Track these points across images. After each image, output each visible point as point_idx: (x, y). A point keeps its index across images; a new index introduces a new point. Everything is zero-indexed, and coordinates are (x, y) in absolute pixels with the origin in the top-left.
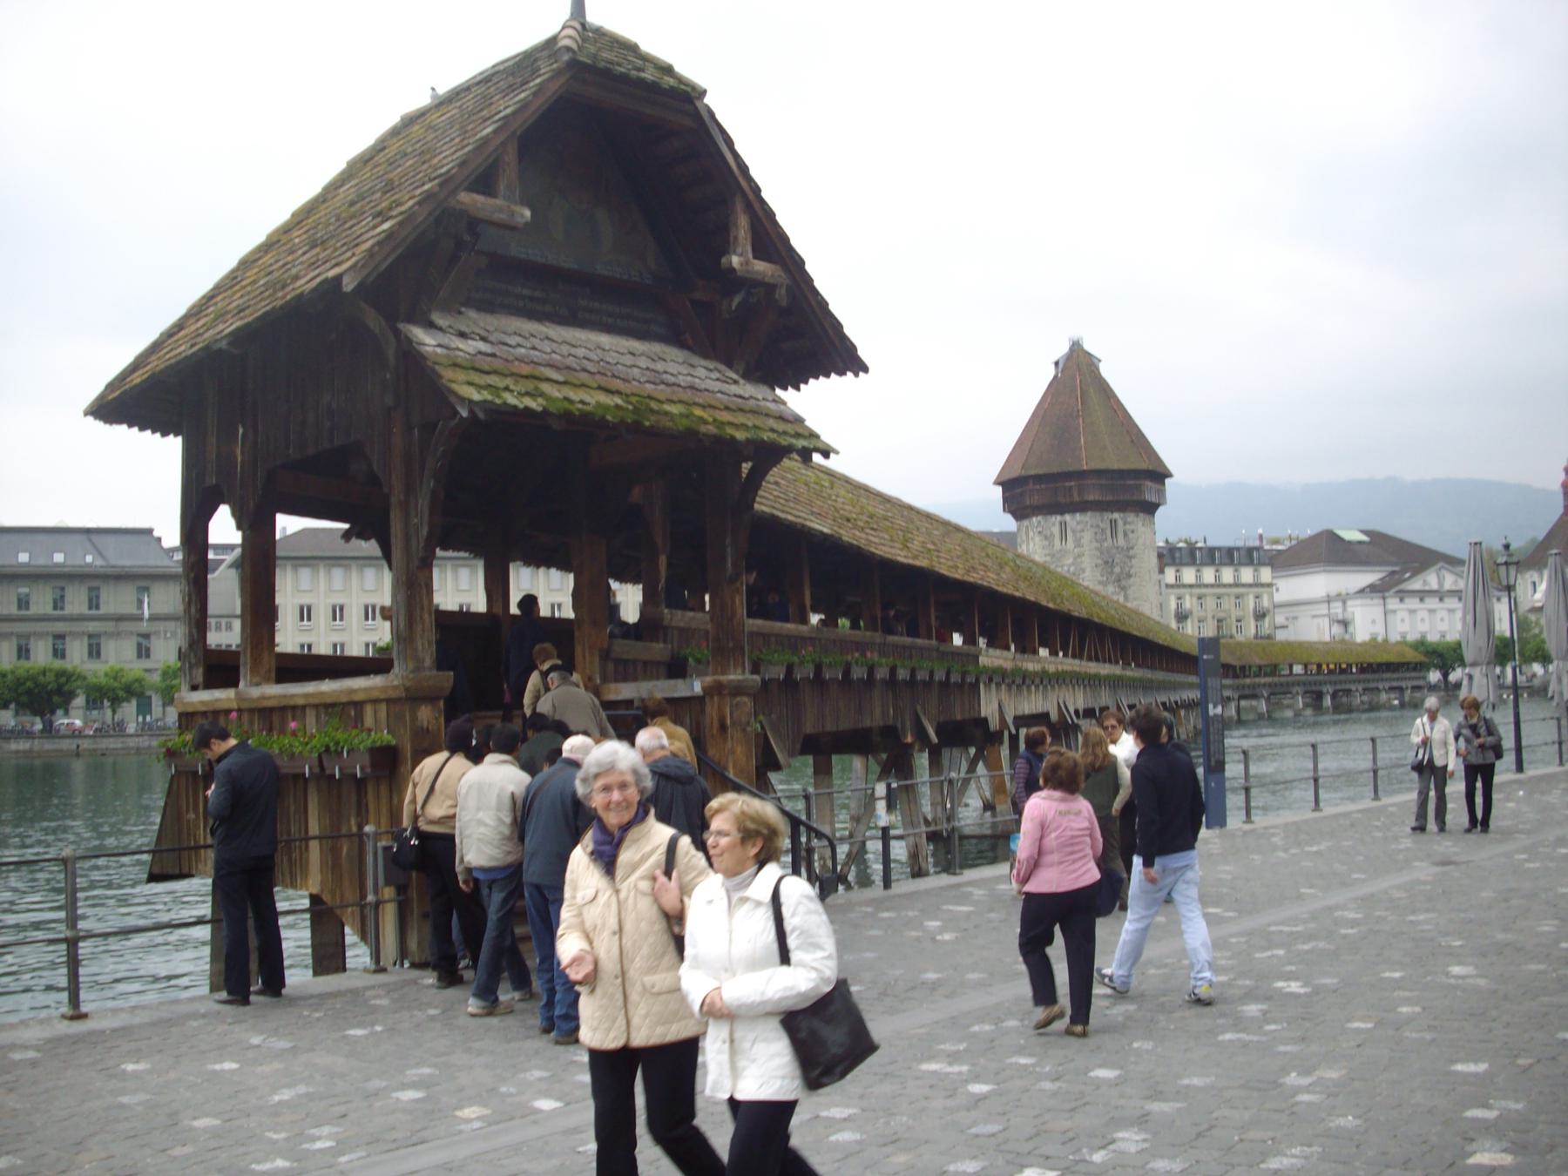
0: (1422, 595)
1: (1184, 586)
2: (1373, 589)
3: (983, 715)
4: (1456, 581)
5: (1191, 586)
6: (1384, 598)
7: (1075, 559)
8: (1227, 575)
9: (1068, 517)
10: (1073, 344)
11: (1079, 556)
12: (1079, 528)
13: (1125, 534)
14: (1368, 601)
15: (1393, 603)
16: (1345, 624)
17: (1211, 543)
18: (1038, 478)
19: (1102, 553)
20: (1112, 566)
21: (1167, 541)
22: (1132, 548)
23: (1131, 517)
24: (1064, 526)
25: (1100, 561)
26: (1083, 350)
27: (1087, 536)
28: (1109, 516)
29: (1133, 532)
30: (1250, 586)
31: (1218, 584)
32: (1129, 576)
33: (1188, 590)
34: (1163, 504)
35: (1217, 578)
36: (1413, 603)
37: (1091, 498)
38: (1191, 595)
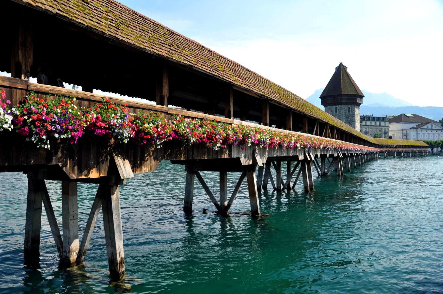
2: (413, 128)
5: (369, 126)
8: (378, 123)
9: (337, 106)
12: (340, 109)
13: (352, 111)
14: (413, 131)
15: (419, 131)
17: (374, 116)
18: (330, 96)
20: (348, 119)
21: (363, 115)
23: (353, 107)
24: (336, 108)
25: (345, 117)
27: (343, 110)
30: (383, 126)
31: (376, 125)
32: (353, 121)
35: (375, 124)
36: (424, 131)
37: (343, 101)
38: (369, 128)
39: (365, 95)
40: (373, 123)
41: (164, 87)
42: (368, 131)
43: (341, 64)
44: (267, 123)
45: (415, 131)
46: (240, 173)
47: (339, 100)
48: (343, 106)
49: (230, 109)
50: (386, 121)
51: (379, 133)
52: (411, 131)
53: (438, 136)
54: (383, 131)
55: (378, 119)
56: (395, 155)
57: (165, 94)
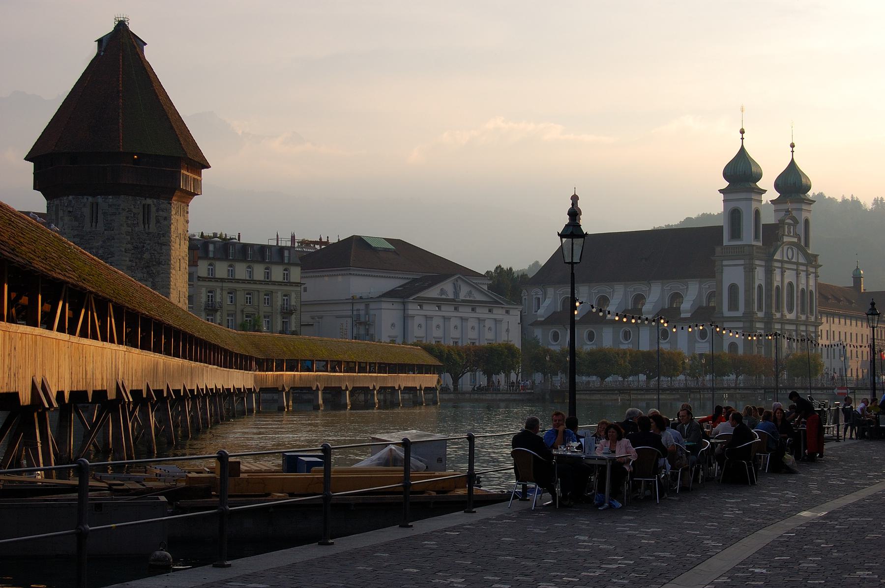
0: (439, 302)
2: (391, 294)
4: (470, 292)
5: (222, 280)
6: (404, 303)
7: (104, 242)
8: (259, 272)
9: (100, 199)
11: (108, 239)
13: (158, 221)
14: (389, 306)
15: (413, 309)
16: (367, 325)
24: (95, 207)
29: (165, 219)
30: (279, 283)
32: (159, 263)
33: (220, 284)
34: (198, 195)
36: (430, 310)
38: (222, 290)
40: (241, 270)
42: (218, 300)
43: (121, 27)
45: (396, 306)
50: (289, 264)
51: (264, 309)
52: (384, 305)
53: (476, 326)
54: (280, 303)
56: (321, 401)
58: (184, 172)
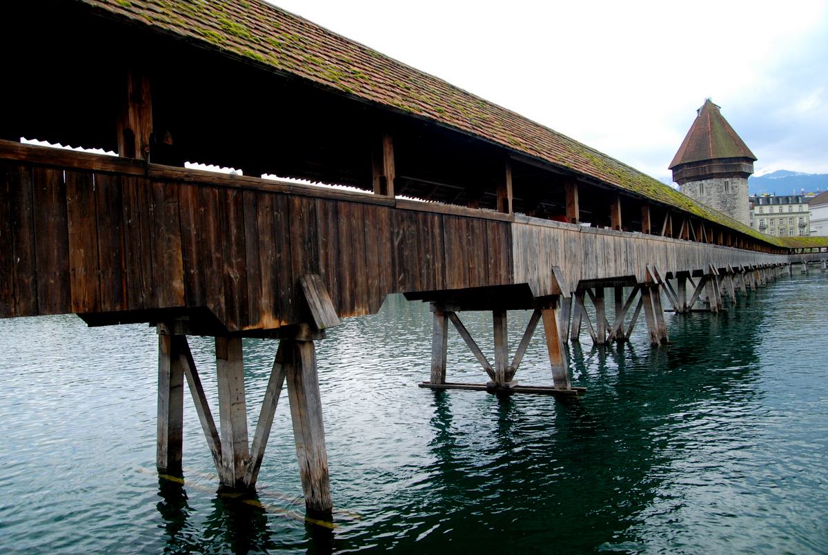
1: (764, 214)
3: (518, 279)
5: (767, 214)
8: (786, 208)
9: (703, 182)
10: (707, 101)
12: (710, 186)
13: (733, 189)
17: (777, 195)
19: (720, 197)
20: (726, 204)
22: (736, 195)
23: (735, 180)
26: (711, 103)
27: (713, 190)
28: (724, 180)
30: (797, 213)
37: (715, 172)
39: (757, 156)
40: (776, 209)
41: (386, 161)
43: (708, 102)
44: (575, 219)
46: (532, 311)
47: (707, 170)
48: (714, 181)
49: (506, 195)
51: (789, 226)
54: (798, 222)
55: (787, 200)
57: (389, 173)
58: (745, 163)
